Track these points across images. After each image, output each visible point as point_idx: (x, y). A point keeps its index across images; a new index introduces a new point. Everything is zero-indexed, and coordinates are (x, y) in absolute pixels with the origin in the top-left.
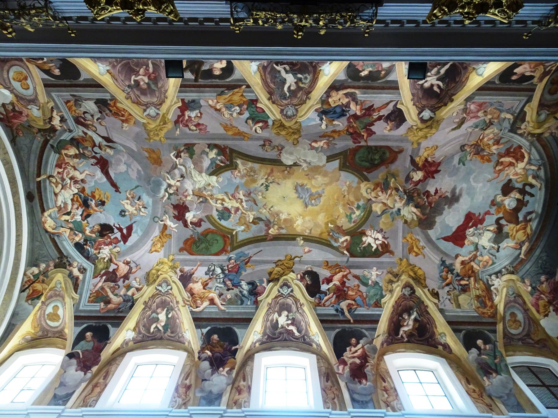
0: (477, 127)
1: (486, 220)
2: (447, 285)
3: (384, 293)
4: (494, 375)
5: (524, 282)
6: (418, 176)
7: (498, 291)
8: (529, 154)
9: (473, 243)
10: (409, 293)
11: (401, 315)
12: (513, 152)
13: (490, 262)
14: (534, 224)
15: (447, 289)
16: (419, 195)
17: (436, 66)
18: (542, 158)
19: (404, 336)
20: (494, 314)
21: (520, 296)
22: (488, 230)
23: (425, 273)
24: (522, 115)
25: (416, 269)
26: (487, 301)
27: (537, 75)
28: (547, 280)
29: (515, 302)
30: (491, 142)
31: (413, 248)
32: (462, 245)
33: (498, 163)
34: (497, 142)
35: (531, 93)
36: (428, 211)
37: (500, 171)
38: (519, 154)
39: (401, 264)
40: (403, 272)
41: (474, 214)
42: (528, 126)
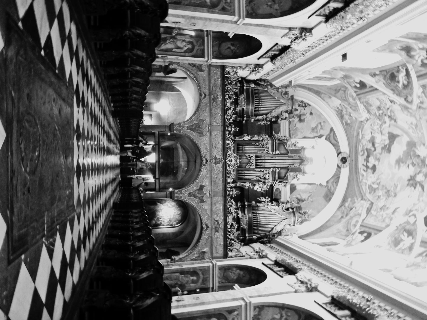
0: (388, 208)
1: (380, 150)
2: (388, 109)
3: (423, 95)
4: (342, 76)
5: (355, 118)
6: (420, 178)
7: (364, 111)
8: (366, 189)
9: (384, 135)
10: (408, 98)
11: (409, 82)
12: (372, 190)
13: (373, 125)
14: (360, 149)
15: (388, 106)
16: (418, 164)
17: (405, 249)
18: (361, 186)
19: (402, 69)
20: (360, 99)
21: (354, 110)
22: (378, 143)
23: (403, 112)
24: (368, 211)
25: (409, 114)
26: (366, 104)
27: (357, 234)
28: (347, 121)
29: (355, 107)
30: (382, 197)
31: (415, 128)
32: (389, 133)
33: (379, 184)
34: (379, 197)
35: (363, 224)
36: (412, 153)
37: (378, 179)
38: (370, 189)
39: (420, 116)
40: (416, 111)
41: (387, 152)
42: (366, 205)
